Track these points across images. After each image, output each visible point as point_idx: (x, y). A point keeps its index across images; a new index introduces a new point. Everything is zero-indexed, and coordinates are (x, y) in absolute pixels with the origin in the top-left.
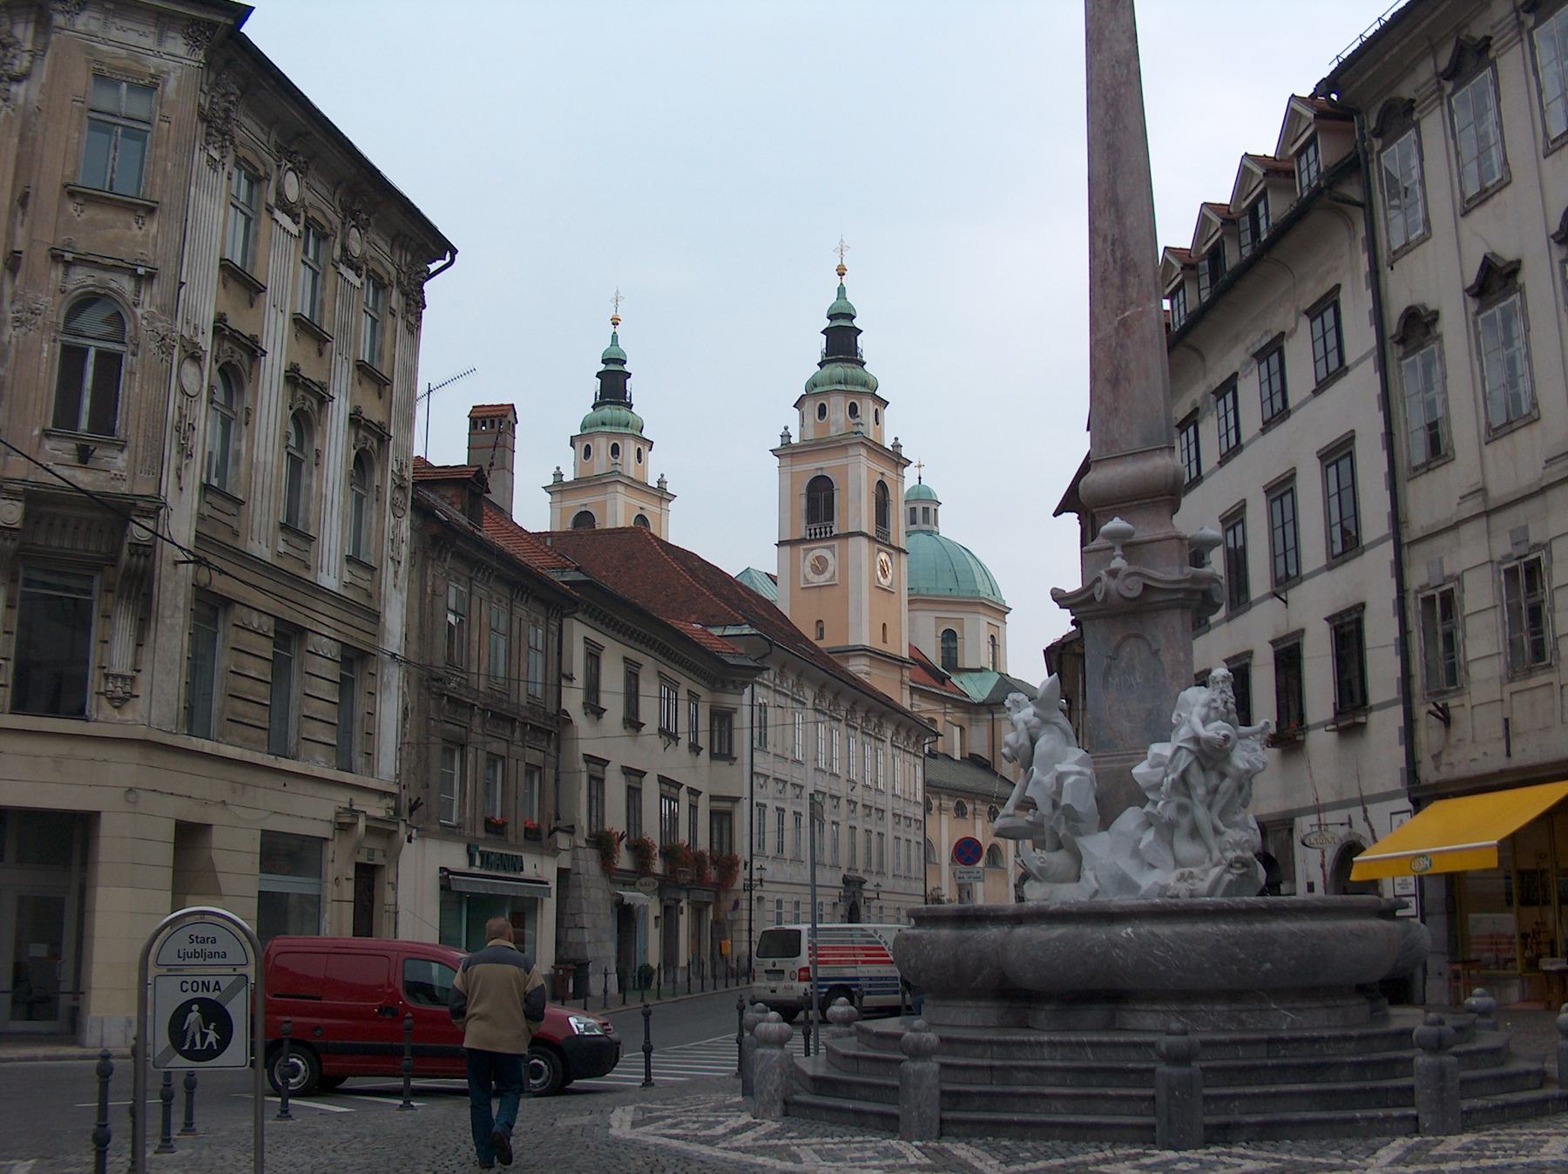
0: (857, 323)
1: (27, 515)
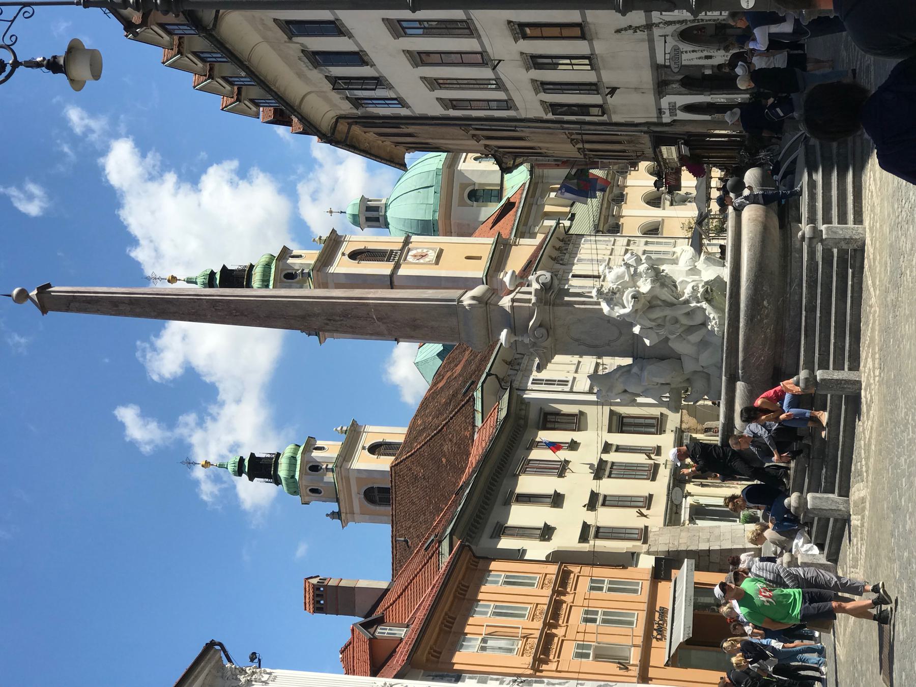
0: (217, 270)
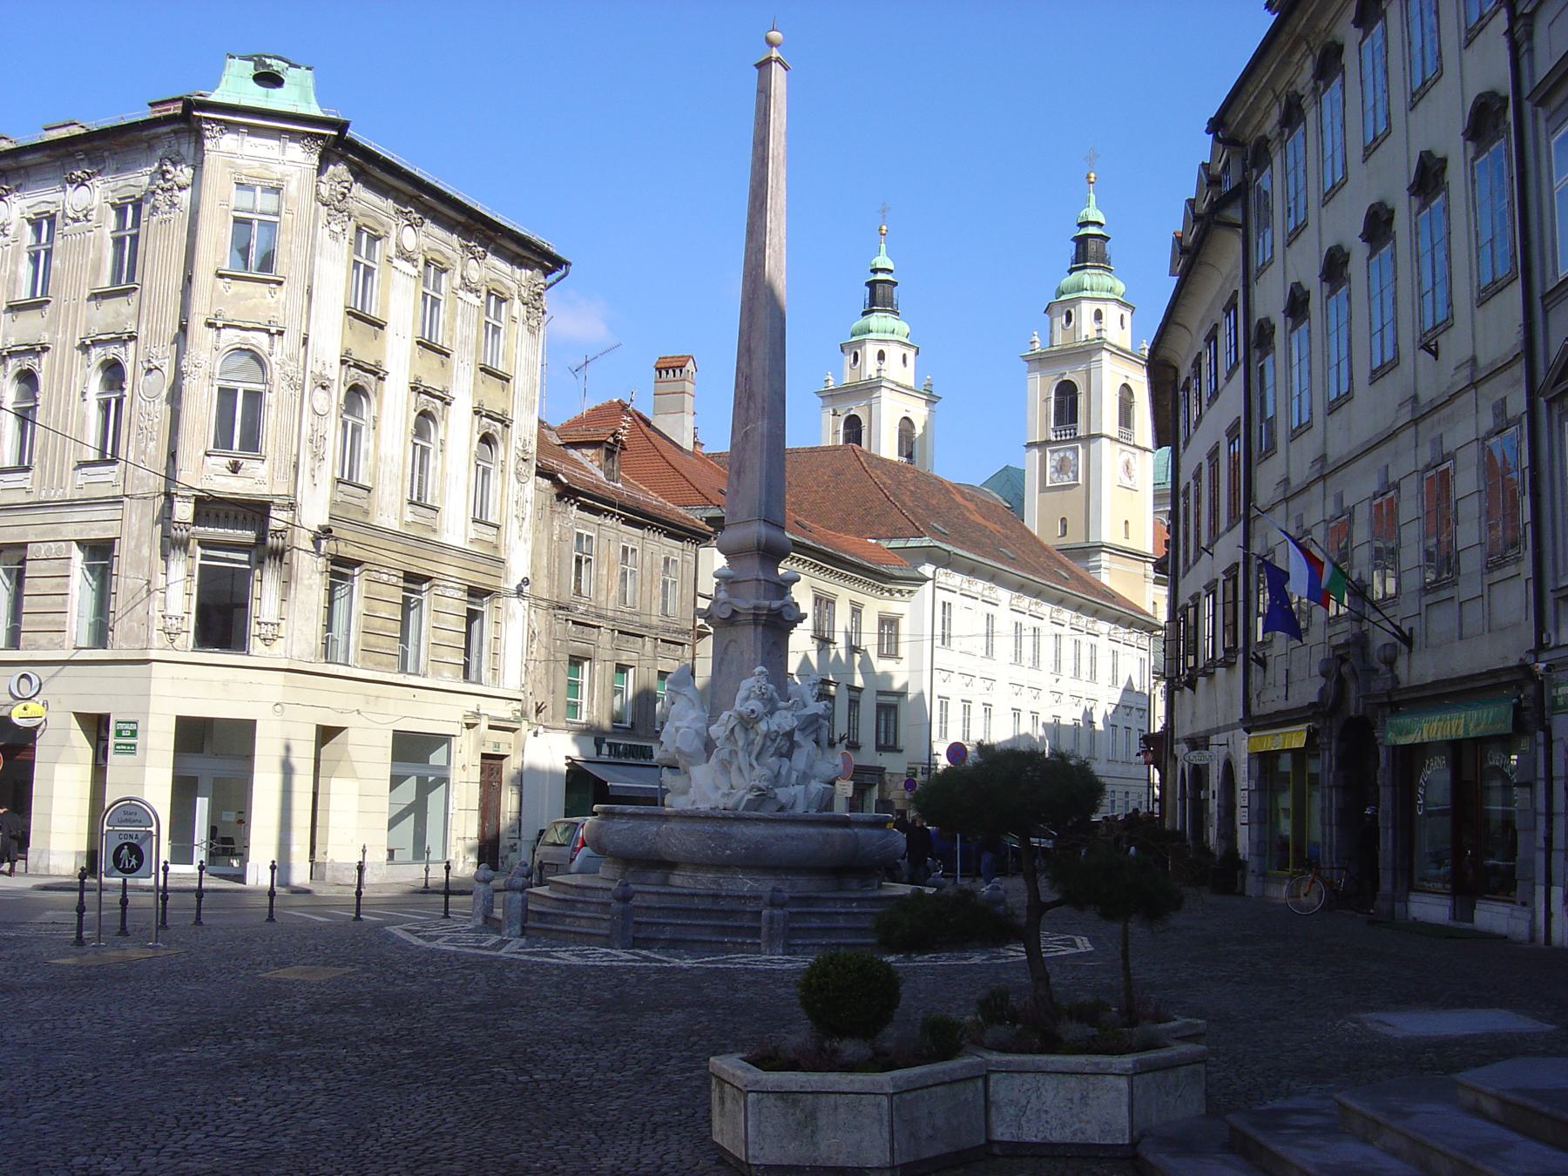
1: (196, 514)
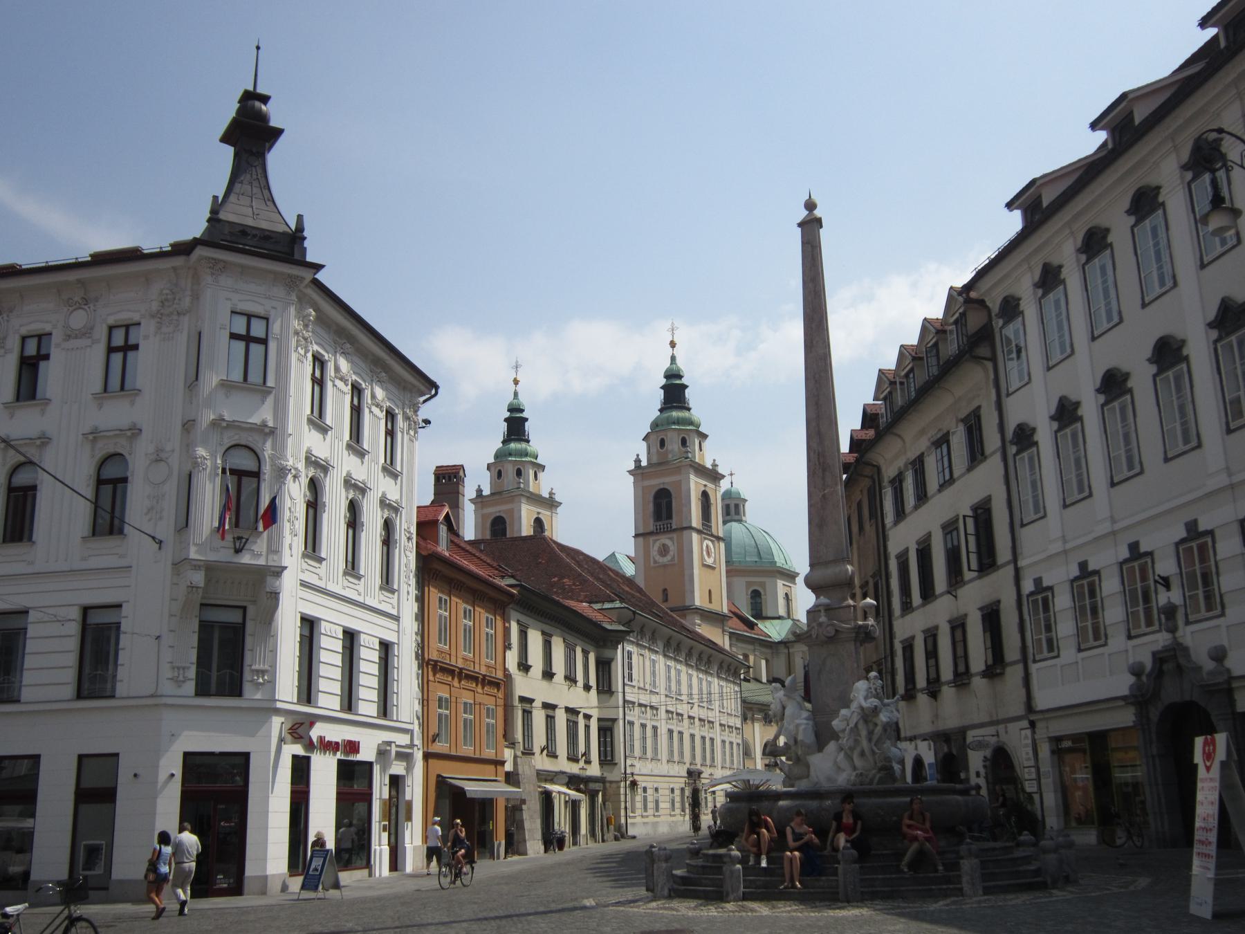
0: (684, 381)
